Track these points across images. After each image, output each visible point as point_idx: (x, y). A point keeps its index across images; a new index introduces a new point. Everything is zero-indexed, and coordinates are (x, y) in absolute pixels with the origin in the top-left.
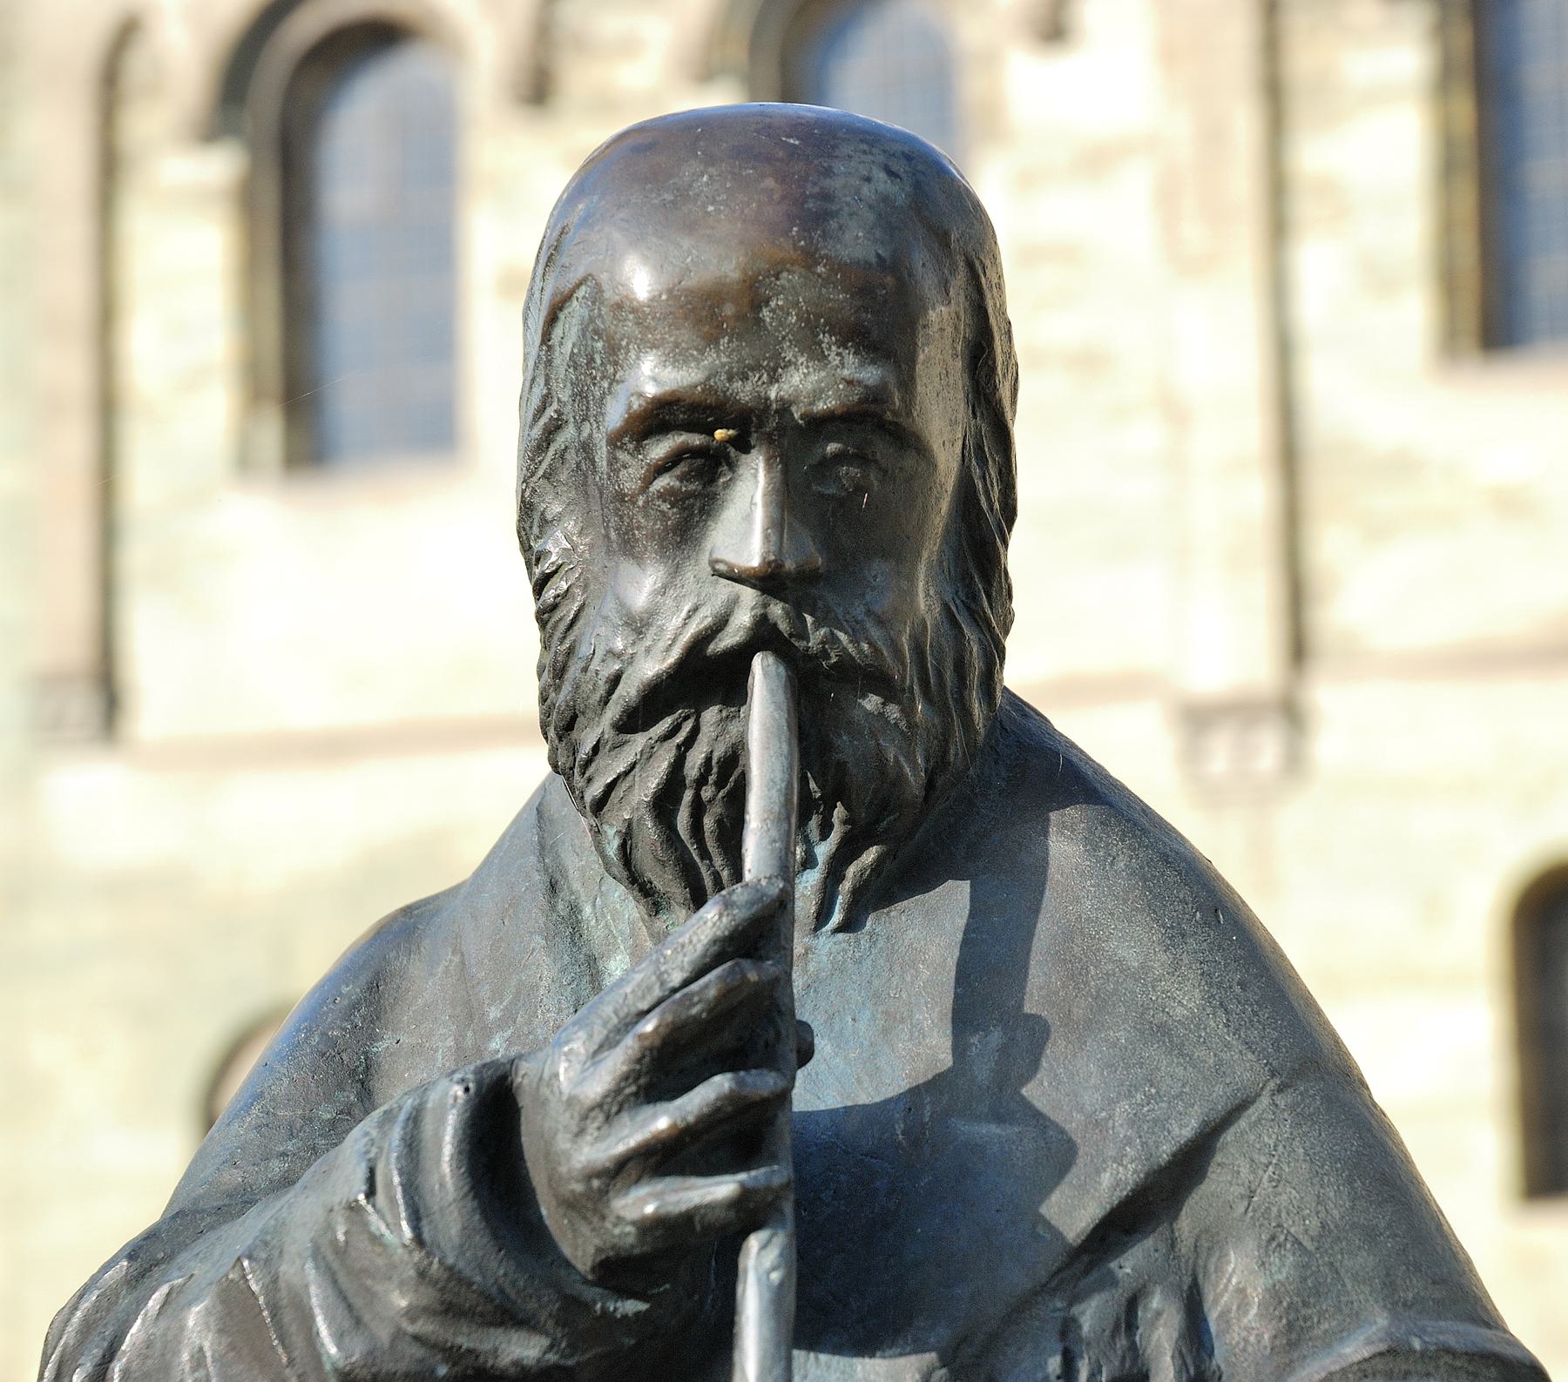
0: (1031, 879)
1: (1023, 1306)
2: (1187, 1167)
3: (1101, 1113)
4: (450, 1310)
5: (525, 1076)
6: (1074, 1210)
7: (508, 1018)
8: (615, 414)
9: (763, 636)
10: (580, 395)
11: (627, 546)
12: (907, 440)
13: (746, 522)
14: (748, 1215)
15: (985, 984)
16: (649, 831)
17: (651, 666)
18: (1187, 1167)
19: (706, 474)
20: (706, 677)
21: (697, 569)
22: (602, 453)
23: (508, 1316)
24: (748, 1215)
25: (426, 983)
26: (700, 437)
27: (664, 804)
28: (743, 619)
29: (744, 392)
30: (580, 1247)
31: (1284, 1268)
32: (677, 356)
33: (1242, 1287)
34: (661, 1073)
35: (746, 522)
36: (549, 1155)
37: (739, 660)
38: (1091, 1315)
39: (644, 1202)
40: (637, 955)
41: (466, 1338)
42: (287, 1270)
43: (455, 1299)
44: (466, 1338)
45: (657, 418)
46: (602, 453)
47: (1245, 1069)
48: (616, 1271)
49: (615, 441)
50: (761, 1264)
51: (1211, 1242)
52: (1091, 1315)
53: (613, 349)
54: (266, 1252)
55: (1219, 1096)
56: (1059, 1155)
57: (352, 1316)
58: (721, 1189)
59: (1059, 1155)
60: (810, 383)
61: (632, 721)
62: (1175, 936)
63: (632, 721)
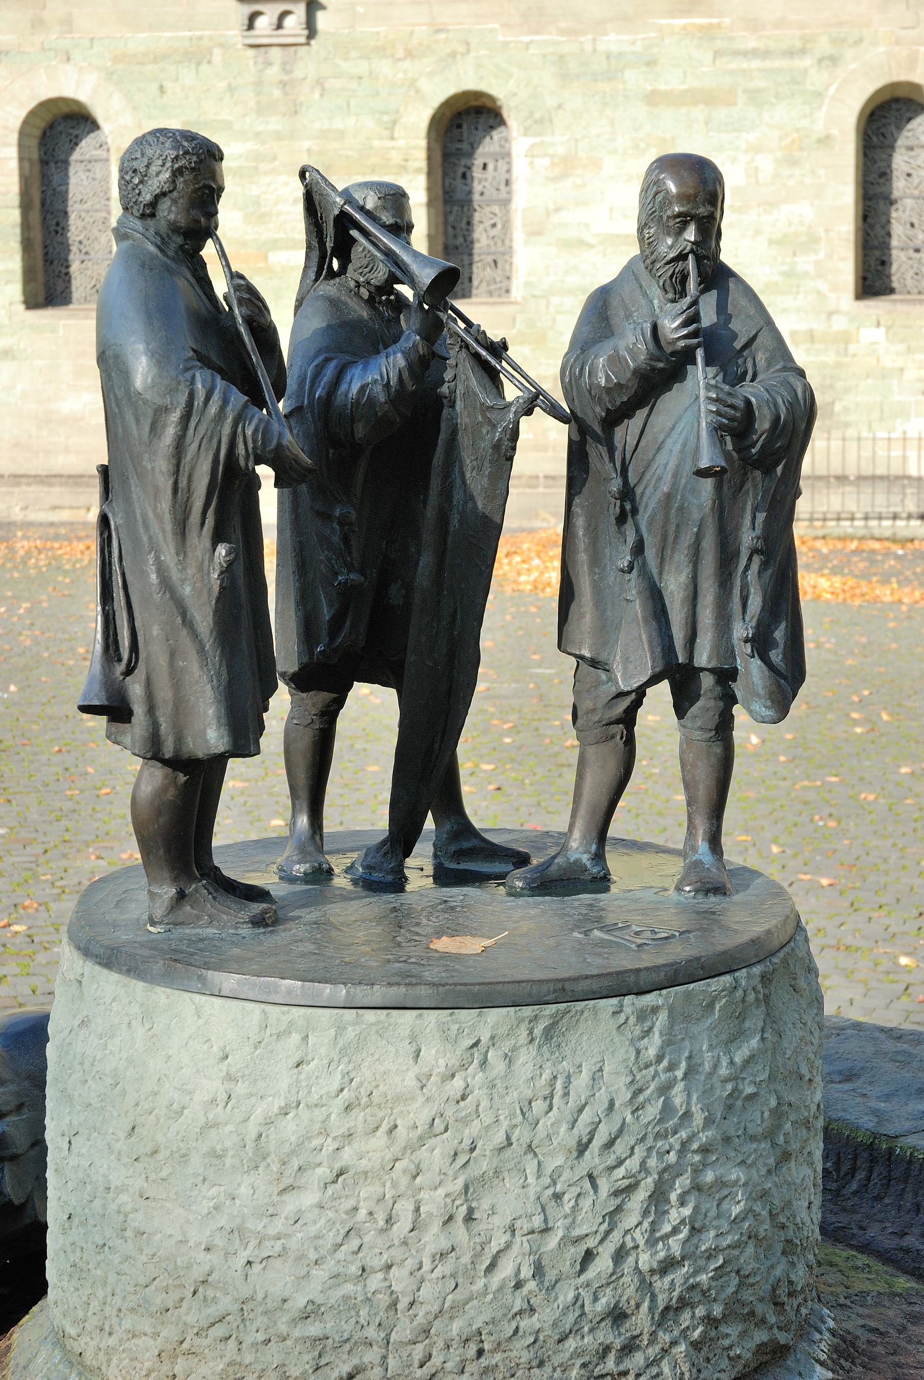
0: (728, 289)
1: (730, 361)
2: (754, 338)
3: (741, 328)
4: (651, 359)
5: (659, 322)
6: (738, 345)
7: (637, 310)
8: (669, 213)
9: (692, 251)
10: (661, 208)
11: (668, 234)
12: (715, 219)
13: (691, 234)
14: (698, 345)
15: (722, 308)
16: (668, 281)
17: (672, 255)
18: (754, 338)
19: (684, 225)
20: (682, 257)
21: (681, 239)
22: (665, 218)
23: (659, 360)
24: (698, 345)
25: (615, 302)
26: (684, 220)
27: (671, 277)
28: (688, 248)
29: (693, 212)
30: (669, 350)
31: (768, 355)
32: (682, 205)
33: (761, 358)
34: (685, 324)
35: (691, 234)
36: (665, 335)
37: (687, 254)
38: (740, 361)
39: (682, 343)
40: (660, 301)
41: (653, 363)
42: (621, 353)
43: (652, 358)
44: (653, 363)
45: (679, 215)
46: (665, 218)
47: (762, 323)
48: (673, 354)
49: (668, 217)
50: (700, 354)
51: (757, 350)
52: (740, 361)
53: (670, 203)
54: (616, 350)
55: (759, 327)
56: (735, 336)
57: (634, 360)
58: (695, 341)
59: (735, 336)
60: (702, 211)
61: (668, 263)
62: (750, 301)
63: (668, 263)
